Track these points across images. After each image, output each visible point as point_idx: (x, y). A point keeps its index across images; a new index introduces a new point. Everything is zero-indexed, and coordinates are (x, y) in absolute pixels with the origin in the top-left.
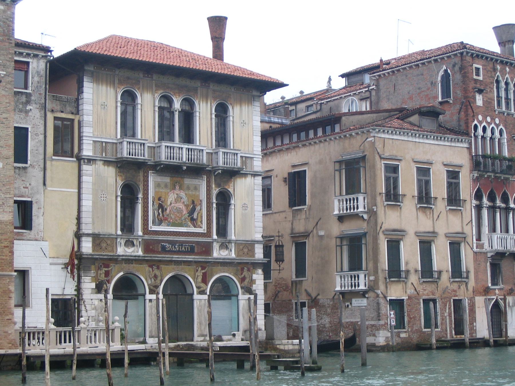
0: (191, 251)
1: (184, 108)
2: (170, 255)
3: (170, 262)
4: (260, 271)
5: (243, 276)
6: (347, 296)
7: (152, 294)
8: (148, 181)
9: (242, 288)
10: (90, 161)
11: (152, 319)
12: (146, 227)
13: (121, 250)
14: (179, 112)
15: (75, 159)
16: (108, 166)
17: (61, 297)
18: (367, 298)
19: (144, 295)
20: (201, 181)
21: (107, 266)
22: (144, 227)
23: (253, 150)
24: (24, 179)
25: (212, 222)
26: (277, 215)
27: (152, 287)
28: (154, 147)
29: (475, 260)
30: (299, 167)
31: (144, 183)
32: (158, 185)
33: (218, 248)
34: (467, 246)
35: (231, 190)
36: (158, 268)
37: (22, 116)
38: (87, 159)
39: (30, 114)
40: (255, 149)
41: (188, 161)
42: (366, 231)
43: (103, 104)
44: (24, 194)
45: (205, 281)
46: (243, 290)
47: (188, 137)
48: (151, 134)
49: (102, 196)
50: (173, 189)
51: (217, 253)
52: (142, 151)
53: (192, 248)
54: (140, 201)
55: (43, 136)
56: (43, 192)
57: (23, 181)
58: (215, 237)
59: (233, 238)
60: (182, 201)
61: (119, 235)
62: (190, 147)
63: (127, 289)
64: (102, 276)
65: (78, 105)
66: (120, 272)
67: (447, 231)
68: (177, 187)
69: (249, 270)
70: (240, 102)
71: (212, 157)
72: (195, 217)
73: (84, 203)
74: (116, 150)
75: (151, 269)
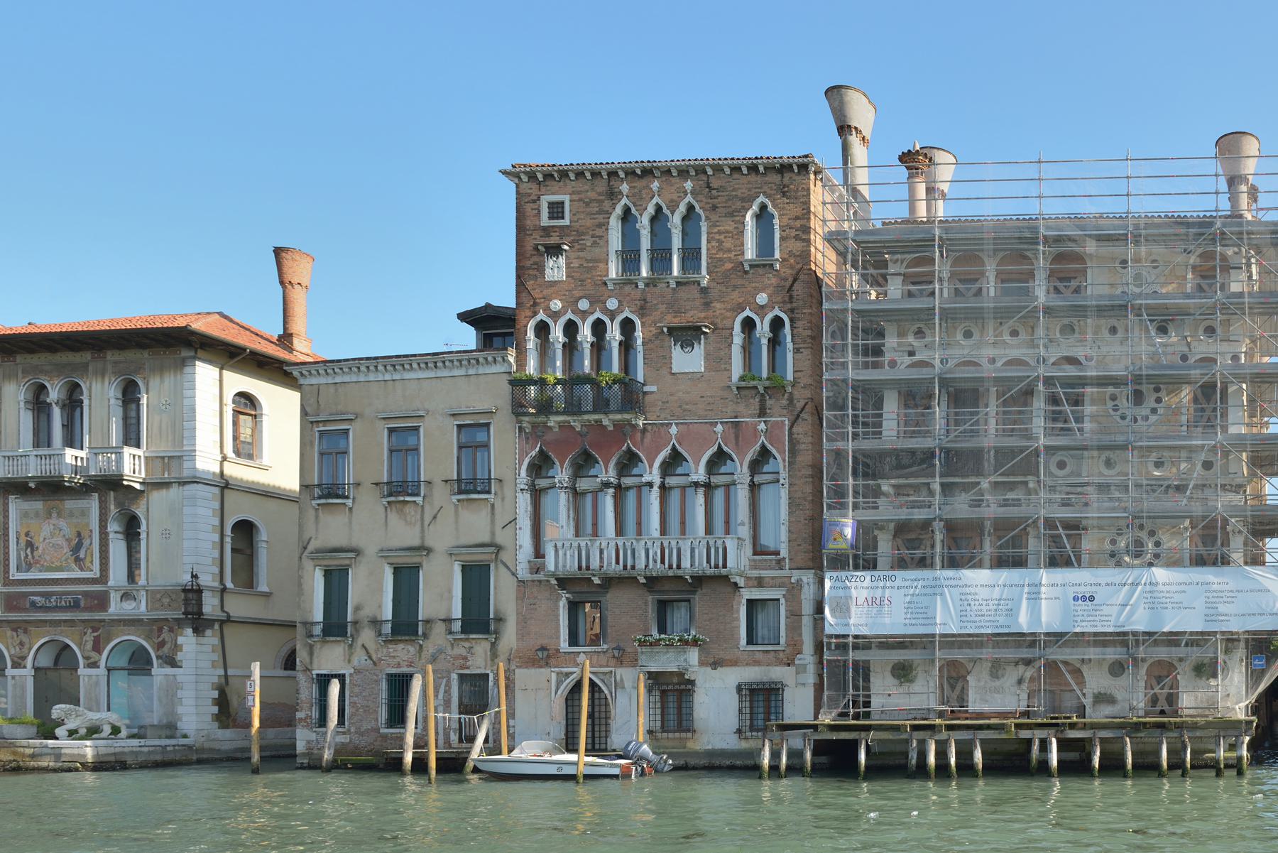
29: (520, 598)
34: (502, 569)
36: (26, 631)
67: (454, 543)
70: (161, 370)
72: (82, 556)
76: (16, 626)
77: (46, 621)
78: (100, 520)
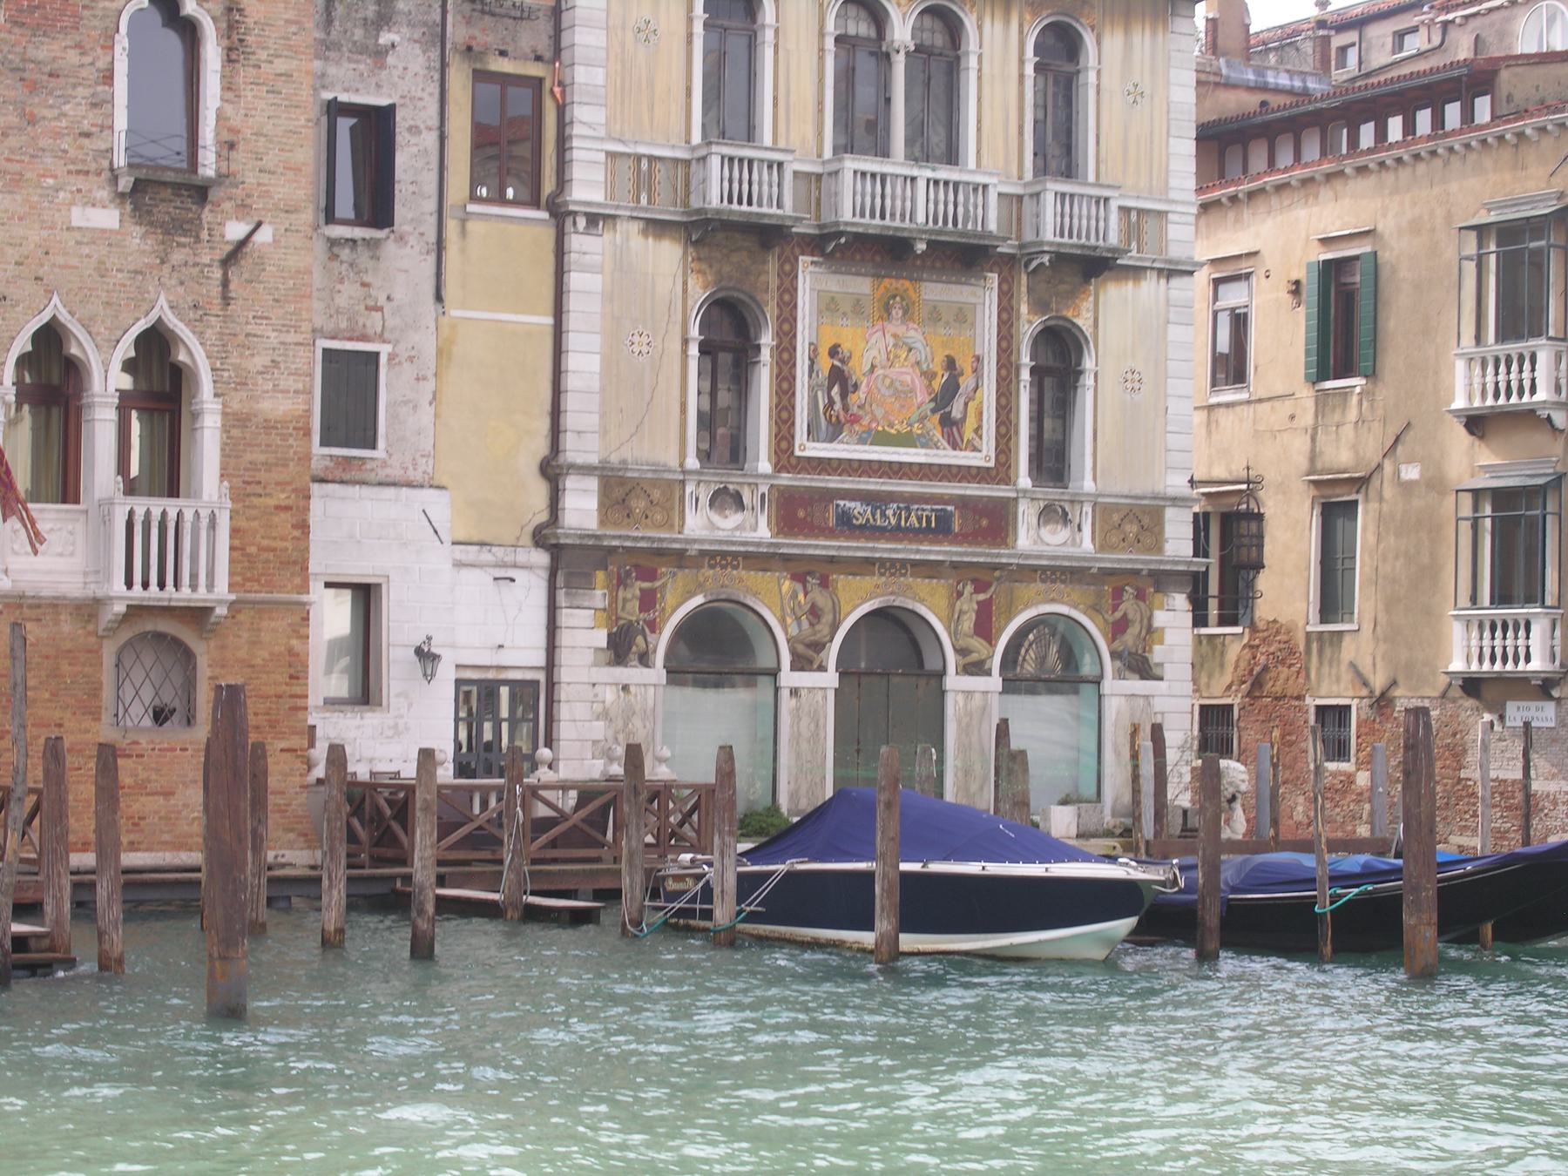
0: (940, 529)
1: (927, 43)
2: (868, 539)
3: (866, 565)
4: (1180, 601)
5: (1118, 615)
6: (1488, 692)
7: (802, 669)
8: (796, 290)
9: (1114, 655)
10: (593, 219)
11: (798, 756)
12: (784, 445)
13: (700, 524)
14: (907, 54)
15: (544, 215)
16: (658, 236)
17: (491, 675)
18: (1558, 700)
19: (774, 673)
20: (980, 291)
21: (650, 575)
22: (778, 444)
23: (1167, 188)
24: (366, 279)
25: (1017, 432)
26: (1266, 406)
27: (800, 648)
28: (819, 177)
30: (1344, 245)
31: (781, 297)
32: (828, 306)
33: (1035, 521)
35: (1084, 322)
36: (824, 583)
37: (362, 67)
38: (586, 214)
39: (390, 60)
40: (1173, 183)
41: (935, 221)
42: (1560, 469)
43: (643, 26)
44: (370, 332)
45: (985, 629)
46: (1118, 664)
47: (939, 137)
48: (809, 130)
49: (636, 339)
50: (881, 317)
51: (1032, 538)
52: (775, 189)
53: (944, 521)
54: (766, 355)
55: (435, 135)
56: (432, 325)
57: (364, 285)
58: (1024, 481)
59: (1088, 485)
60: (912, 358)
61: (691, 472)
62: (944, 173)
63: (717, 650)
64: (629, 606)
65: (558, 31)
66: (691, 595)
68: (897, 313)
69: (1140, 596)
71: (1020, 209)
72: (956, 413)
73: (572, 362)
74: (687, 185)
75: (799, 587)
76: (803, 570)
77: (870, 562)
78: (1000, 339)
